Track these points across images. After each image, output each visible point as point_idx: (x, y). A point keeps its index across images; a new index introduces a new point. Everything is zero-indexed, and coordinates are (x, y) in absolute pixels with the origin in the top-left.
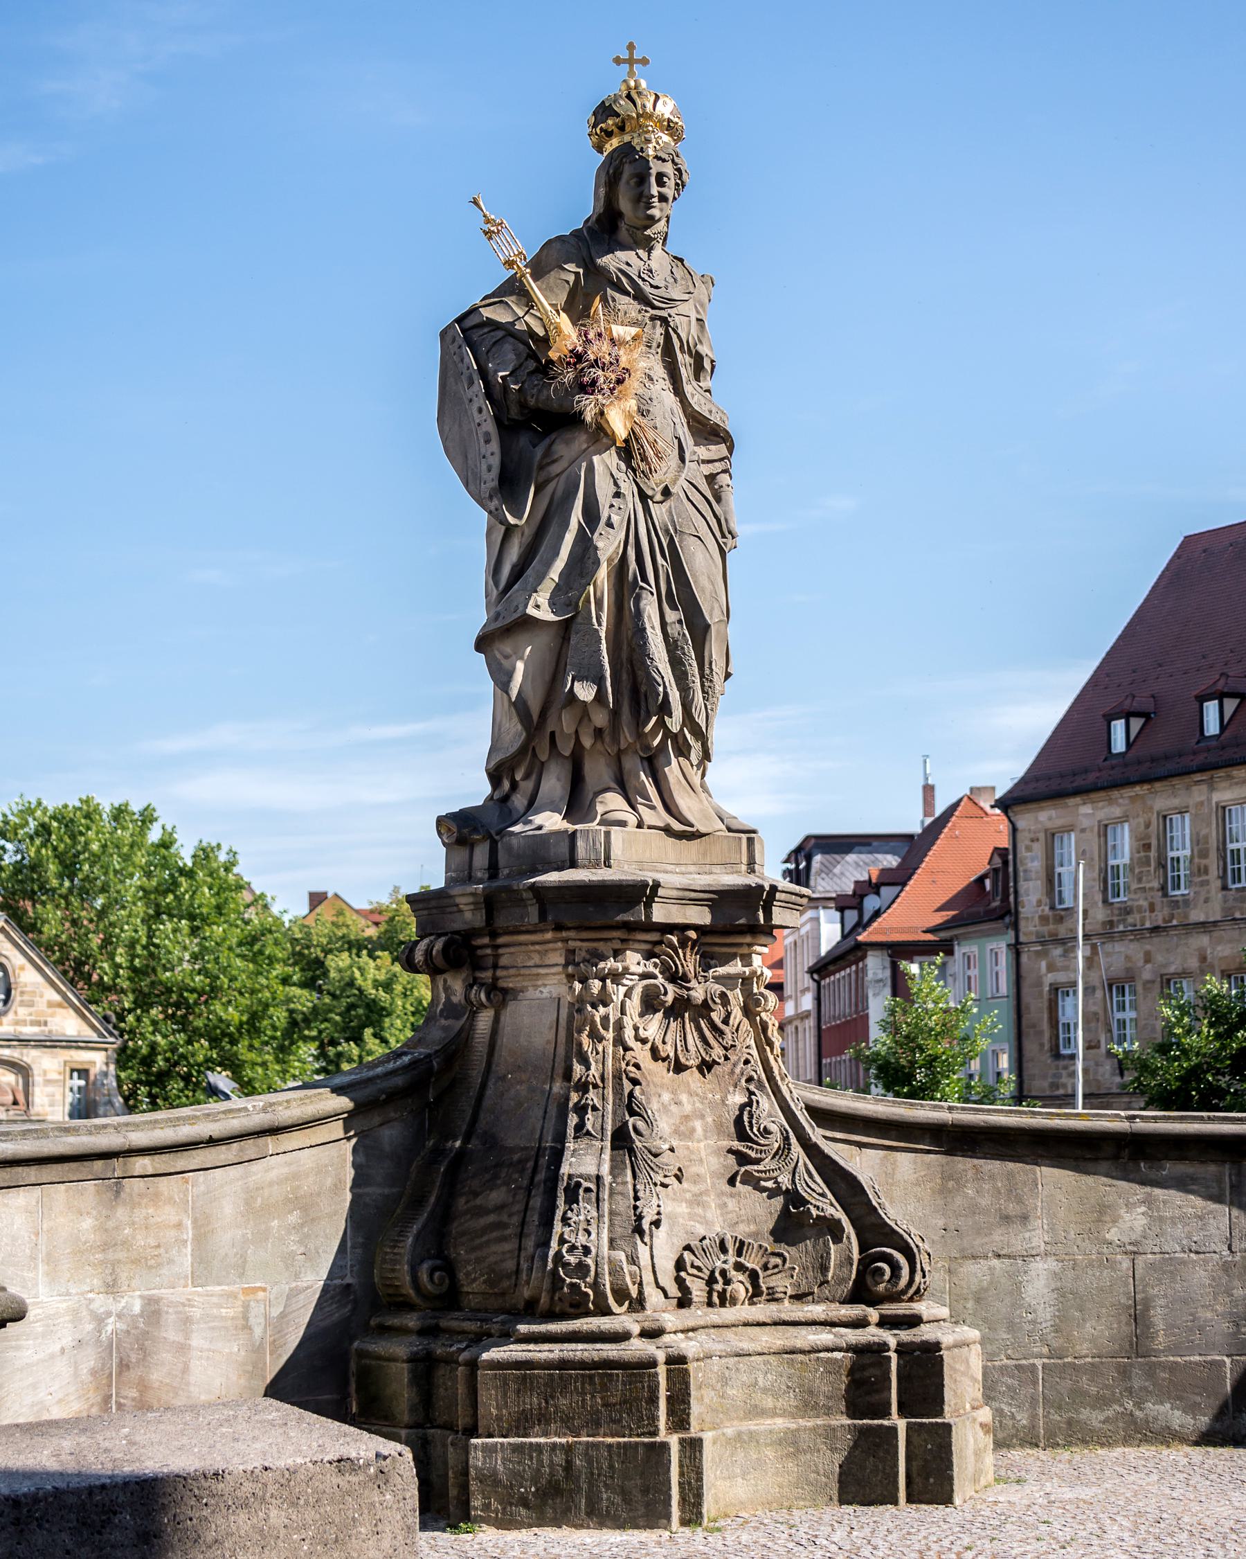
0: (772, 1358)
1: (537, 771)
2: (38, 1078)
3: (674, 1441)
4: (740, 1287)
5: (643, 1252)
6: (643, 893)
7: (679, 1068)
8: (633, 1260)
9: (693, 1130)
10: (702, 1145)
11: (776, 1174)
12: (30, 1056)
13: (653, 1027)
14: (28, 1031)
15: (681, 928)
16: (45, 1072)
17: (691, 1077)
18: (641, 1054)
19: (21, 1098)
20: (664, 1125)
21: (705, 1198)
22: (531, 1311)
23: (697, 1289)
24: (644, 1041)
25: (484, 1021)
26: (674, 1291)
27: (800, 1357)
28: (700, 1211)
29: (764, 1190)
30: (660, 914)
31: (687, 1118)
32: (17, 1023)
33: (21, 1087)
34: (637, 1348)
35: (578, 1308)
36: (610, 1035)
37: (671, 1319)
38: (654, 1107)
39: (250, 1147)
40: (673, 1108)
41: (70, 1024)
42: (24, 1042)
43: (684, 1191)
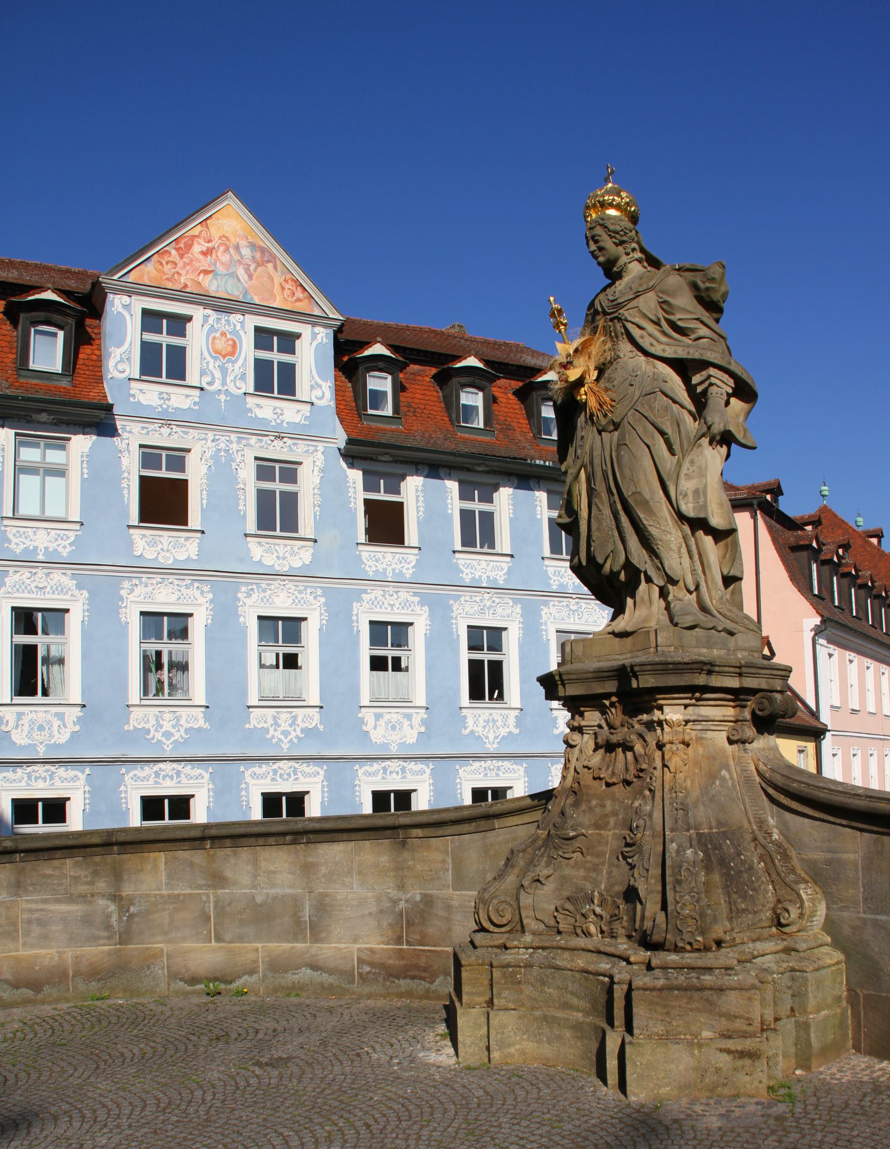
0: (577, 975)
9: (608, 823)
10: (611, 833)
11: (631, 854)
13: (596, 759)
17: (619, 790)
18: (587, 778)
21: (601, 867)
24: (589, 768)
26: (552, 922)
27: (591, 977)
28: (594, 875)
29: (628, 864)
31: (606, 815)
40: (598, 810)
43: (586, 862)
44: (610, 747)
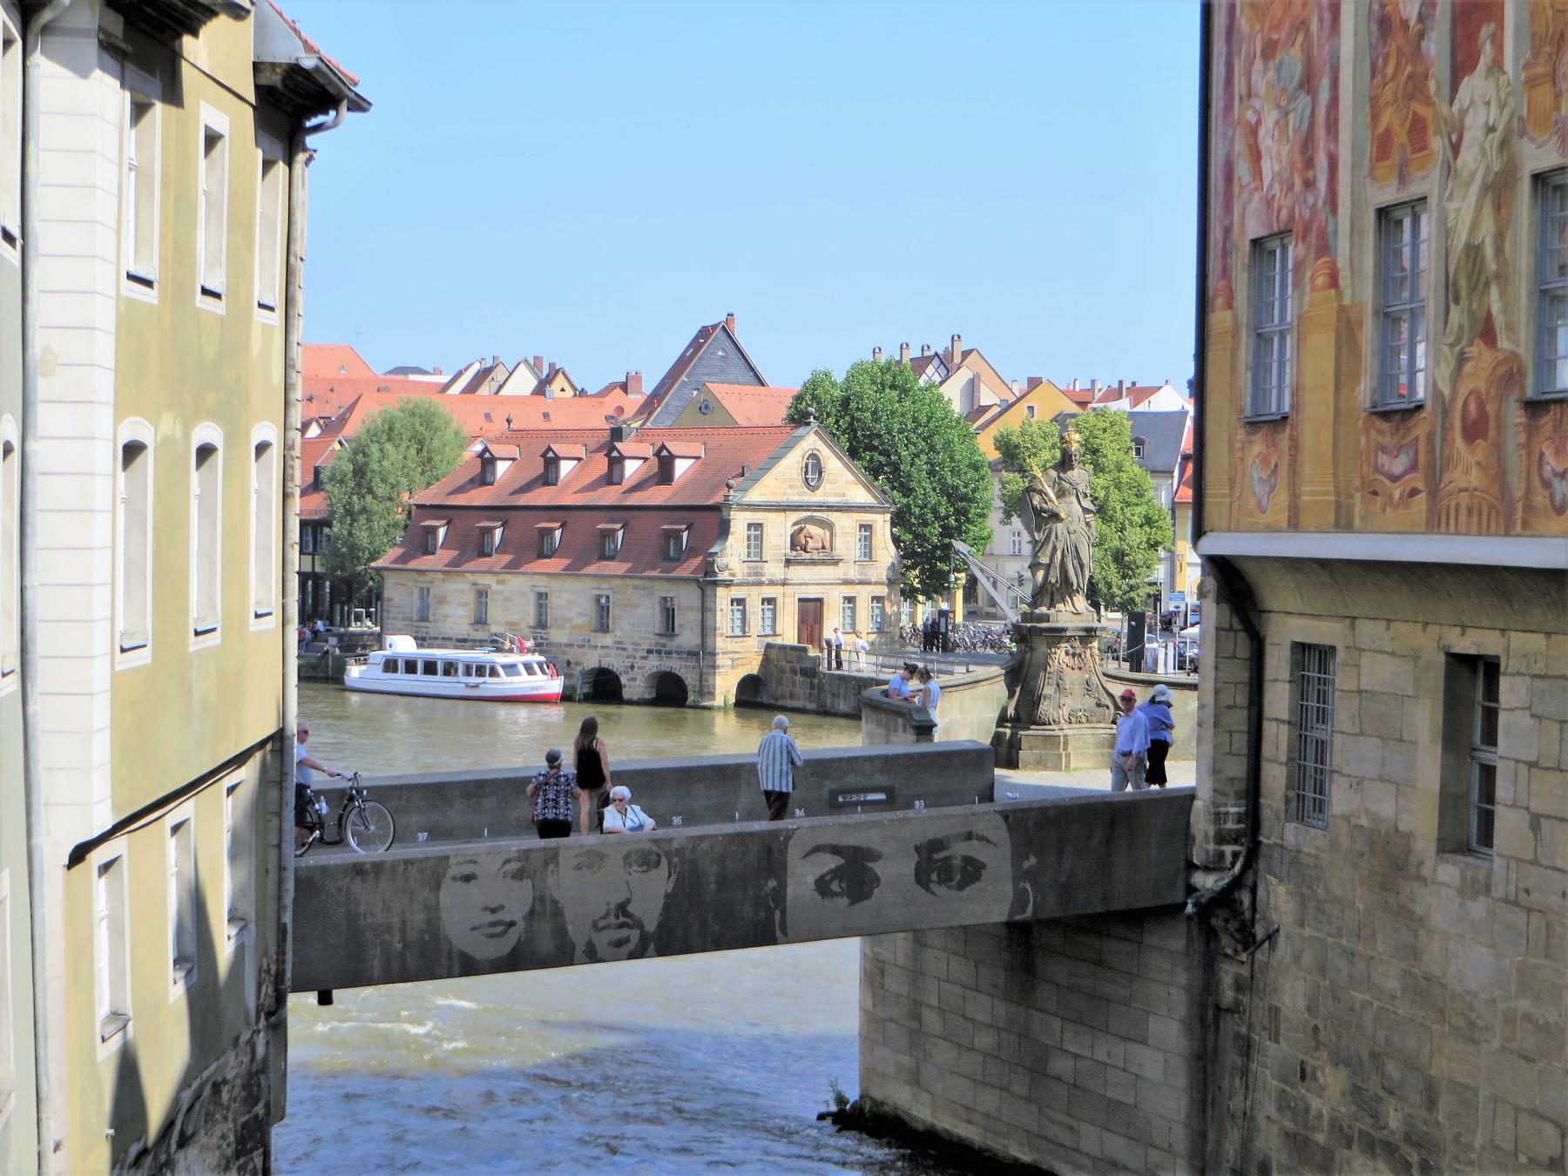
1: (1042, 596)
2: (838, 530)
3: (1064, 753)
4: (1084, 720)
5: (1061, 712)
6: (1064, 630)
7: (1073, 669)
8: (1058, 713)
12: (833, 517)
13: (1067, 659)
14: (832, 500)
15: (1074, 637)
16: (843, 527)
17: (1077, 671)
18: (1064, 666)
19: (827, 545)
20: (1068, 682)
22: (1035, 723)
23: (1073, 720)
25: (1028, 655)
30: (1068, 634)
32: (825, 494)
33: (828, 537)
34: (1057, 733)
35: (1044, 724)
36: (1056, 661)
37: (1065, 726)
38: (1066, 679)
39: (973, 685)
41: (861, 496)
42: (830, 508)
44: (1074, 655)
